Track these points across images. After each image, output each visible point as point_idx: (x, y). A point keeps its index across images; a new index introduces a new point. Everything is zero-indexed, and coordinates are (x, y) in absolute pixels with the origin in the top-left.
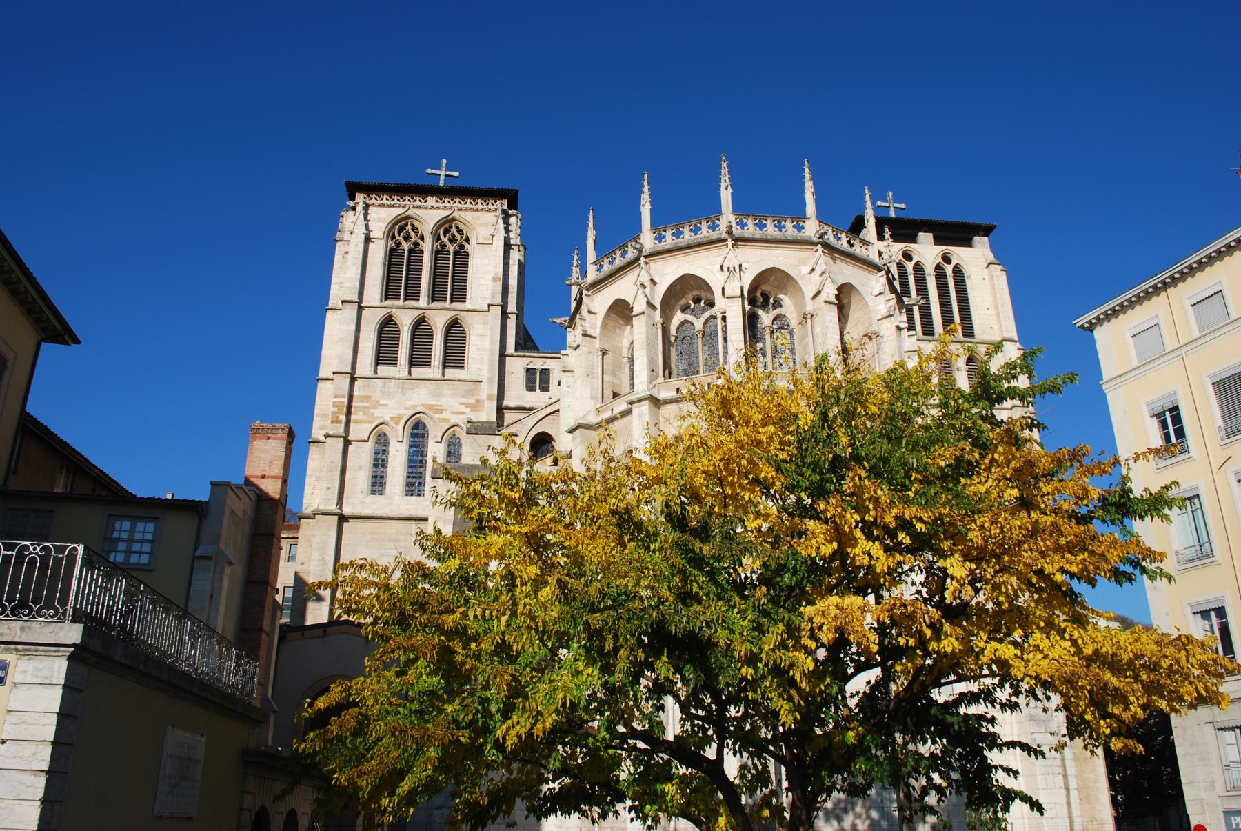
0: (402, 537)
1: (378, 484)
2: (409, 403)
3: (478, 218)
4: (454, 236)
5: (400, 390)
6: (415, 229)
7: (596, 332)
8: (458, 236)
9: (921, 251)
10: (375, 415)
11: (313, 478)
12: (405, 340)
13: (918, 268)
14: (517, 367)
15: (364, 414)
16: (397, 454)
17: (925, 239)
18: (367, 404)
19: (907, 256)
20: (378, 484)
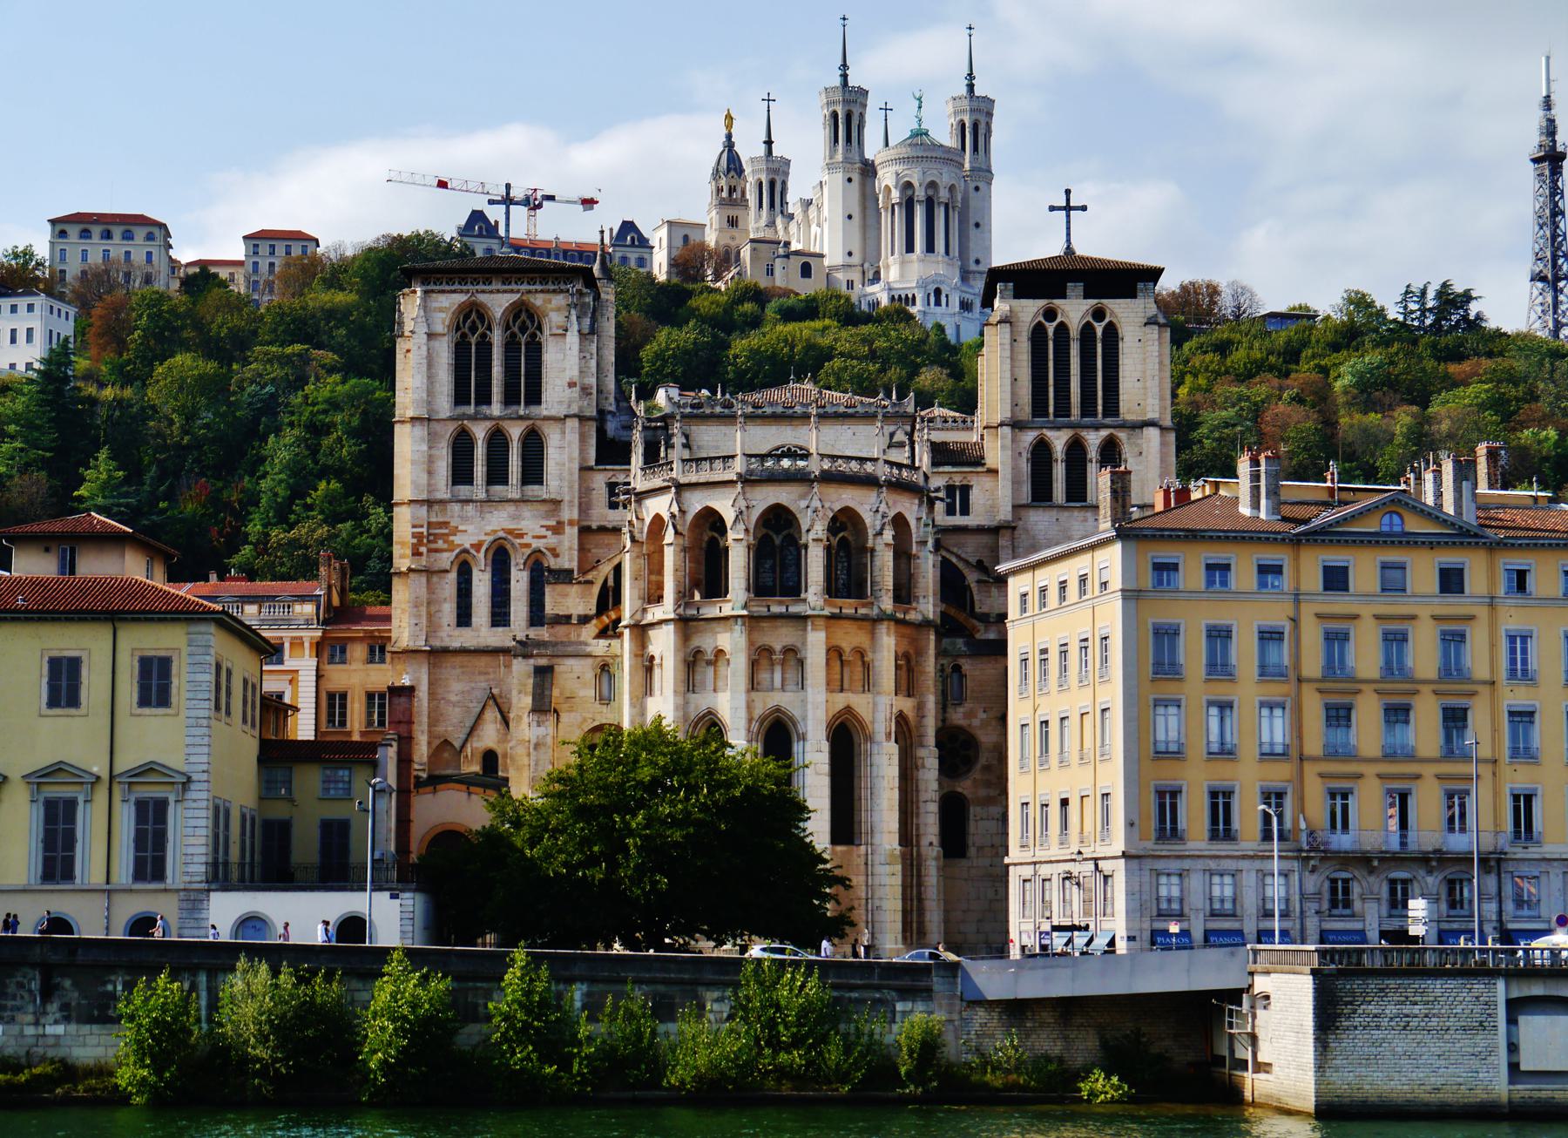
1: (464, 617)
2: (489, 528)
3: (550, 301)
4: (524, 322)
6: (481, 317)
7: (642, 535)
8: (528, 323)
9: (1067, 308)
11: (399, 611)
12: (480, 457)
13: (1062, 329)
14: (599, 481)
15: (445, 542)
18: (446, 531)
19: (1050, 314)
20: (464, 617)
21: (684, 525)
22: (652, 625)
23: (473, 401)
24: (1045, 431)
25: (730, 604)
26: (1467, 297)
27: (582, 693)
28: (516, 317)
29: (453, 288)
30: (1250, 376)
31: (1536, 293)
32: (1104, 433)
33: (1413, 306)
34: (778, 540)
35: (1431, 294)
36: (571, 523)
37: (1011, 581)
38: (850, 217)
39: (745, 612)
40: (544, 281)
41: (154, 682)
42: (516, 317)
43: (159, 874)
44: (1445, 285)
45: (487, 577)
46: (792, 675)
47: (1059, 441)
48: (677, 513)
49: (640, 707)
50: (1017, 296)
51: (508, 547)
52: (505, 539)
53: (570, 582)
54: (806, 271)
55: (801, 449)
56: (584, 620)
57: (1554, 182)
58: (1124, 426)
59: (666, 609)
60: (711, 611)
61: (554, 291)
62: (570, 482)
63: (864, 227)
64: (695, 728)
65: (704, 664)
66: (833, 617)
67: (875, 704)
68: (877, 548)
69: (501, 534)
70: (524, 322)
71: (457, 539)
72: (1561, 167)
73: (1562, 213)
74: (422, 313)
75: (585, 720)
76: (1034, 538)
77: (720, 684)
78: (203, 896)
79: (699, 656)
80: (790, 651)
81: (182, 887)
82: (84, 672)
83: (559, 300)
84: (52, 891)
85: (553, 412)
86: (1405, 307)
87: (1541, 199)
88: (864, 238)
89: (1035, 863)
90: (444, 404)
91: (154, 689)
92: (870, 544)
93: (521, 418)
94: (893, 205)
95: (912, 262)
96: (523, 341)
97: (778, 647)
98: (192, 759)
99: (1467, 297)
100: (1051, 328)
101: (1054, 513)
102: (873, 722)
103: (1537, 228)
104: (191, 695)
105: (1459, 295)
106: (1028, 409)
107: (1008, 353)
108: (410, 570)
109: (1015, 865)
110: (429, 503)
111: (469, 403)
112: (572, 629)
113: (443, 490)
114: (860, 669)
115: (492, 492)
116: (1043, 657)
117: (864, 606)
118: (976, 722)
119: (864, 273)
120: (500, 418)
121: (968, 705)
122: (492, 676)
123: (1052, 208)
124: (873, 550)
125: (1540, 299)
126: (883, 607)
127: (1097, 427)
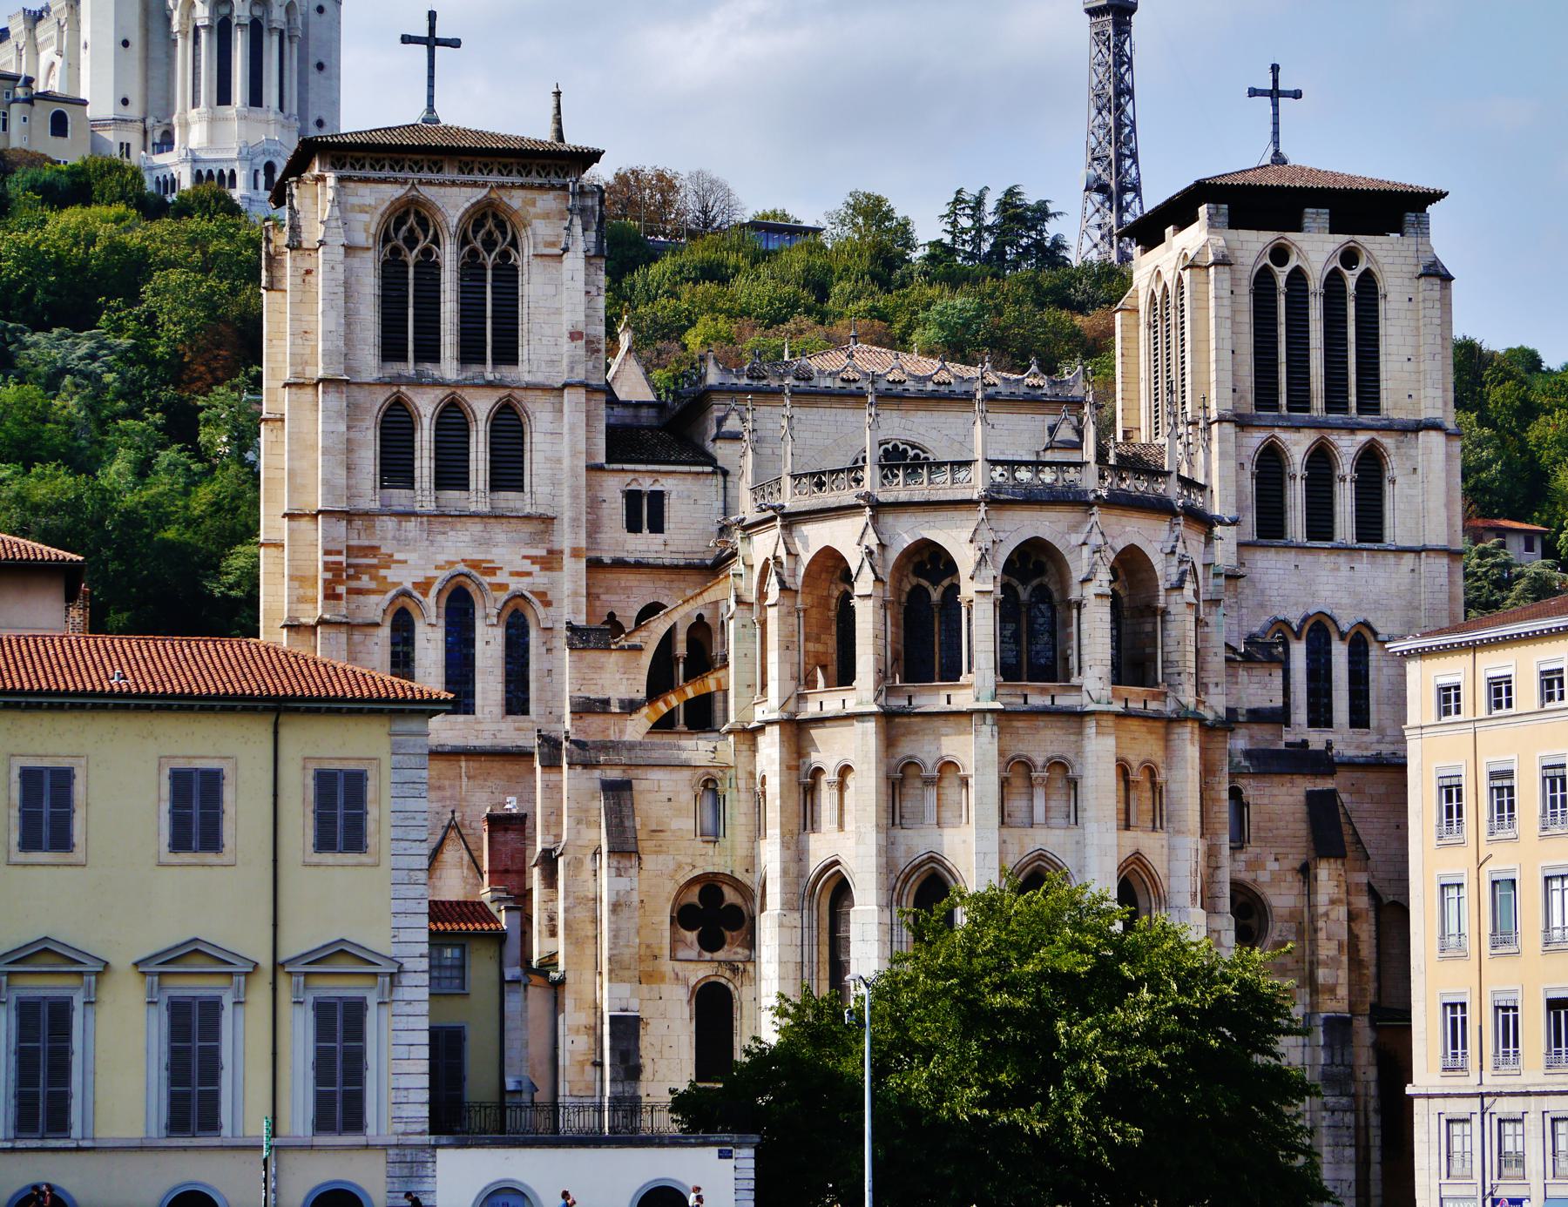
0: (447, 783)
2: (441, 559)
3: (534, 204)
4: (490, 233)
5: (425, 535)
6: (423, 223)
8: (497, 235)
9: (1305, 246)
10: (389, 580)
12: (426, 445)
13: (1298, 276)
14: (614, 487)
15: (372, 578)
16: (429, 645)
17: (1314, 220)
19: (1280, 254)
21: (884, 567)
22: (820, 721)
23: (411, 355)
24: (1277, 432)
25: (969, 691)
26: (1042, 213)
27: (675, 824)
28: (478, 225)
29: (382, 174)
30: (776, 320)
31: (1091, 209)
32: (1362, 438)
33: (966, 223)
34: (1024, 594)
35: (990, 204)
36: (576, 553)
37: (1413, 668)
38: (126, 44)
39: (998, 705)
40: (525, 170)
41: (340, 811)
42: (478, 225)
43: (354, 1121)
44: (1011, 193)
45: (439, 635)
46: (1058, 802)
47: (1297, 446)
48: (874, 548)
49: (796, 851)
50: (1233, 224)
51: (472, 588)
52: (467, 576)
53: (608, 648)
54: (59, 125)
55: (913, 447)
56: (630, 707)
57: (1119, 46)
58: (1389, 428)
59: (863, 693)
60: (933, 699)
61: (541, 187)
62: (574, 488)
63: (147, 60)
64: (905, 881)
65: (918, 783)
66: (1126, 715)
67: (1171, 848)
68: (1172, 609)
69: (462, 568)
70: (490, 233)
71: (391, 575)
72: (1129, 23)
73: (1130, 92)
74: (337, 213)
75: (679, 866)
76: (1263, 591)
77: (947, 815)
78: (422, 1156)
79: (911, 771)
80: (1058, 765)
81: (394, 1140)
82: (228, 795)
83: (548, 202)
84: (185, 1148)
85: (539, 378)
86: (954, 224)
87: (1101, 70)
88: (146, 79)
89: (1482, 1095)
90: (369, 362)
91: (340, 822)
92: (1161, 603)
93: (490, 385)
94: (196, 29)
95: (226, 119)
96: (489, 263)
97: (1039, 760)
98: (404, 936)
99: (1042, 213)
100: (1282, 275)
101: (1291, 556)
102: (1169, 877)
103: (1094, 112)
104: (399, 833)
105: (1028, 208)
106: (1250, 397)
107: (1227, 312)
108: (322, 622)
109: (1429, 1096)
110: (348, 516)
111: (405, 359)
112: (610, 720)
113: (369, 498)
114: (1149, 794)
115: (443, 502)
116: (1498, 783)
117: (1155, 697)
118: (1264, 876)
119: (145, 132)
120: (457, 384)
121: (1252, 850)
122: (448, 794)
123: (1253, 93)
124: (1165, 612)
125: (1096, 219)
126: (1184, 700)
127: (1352, 429)
